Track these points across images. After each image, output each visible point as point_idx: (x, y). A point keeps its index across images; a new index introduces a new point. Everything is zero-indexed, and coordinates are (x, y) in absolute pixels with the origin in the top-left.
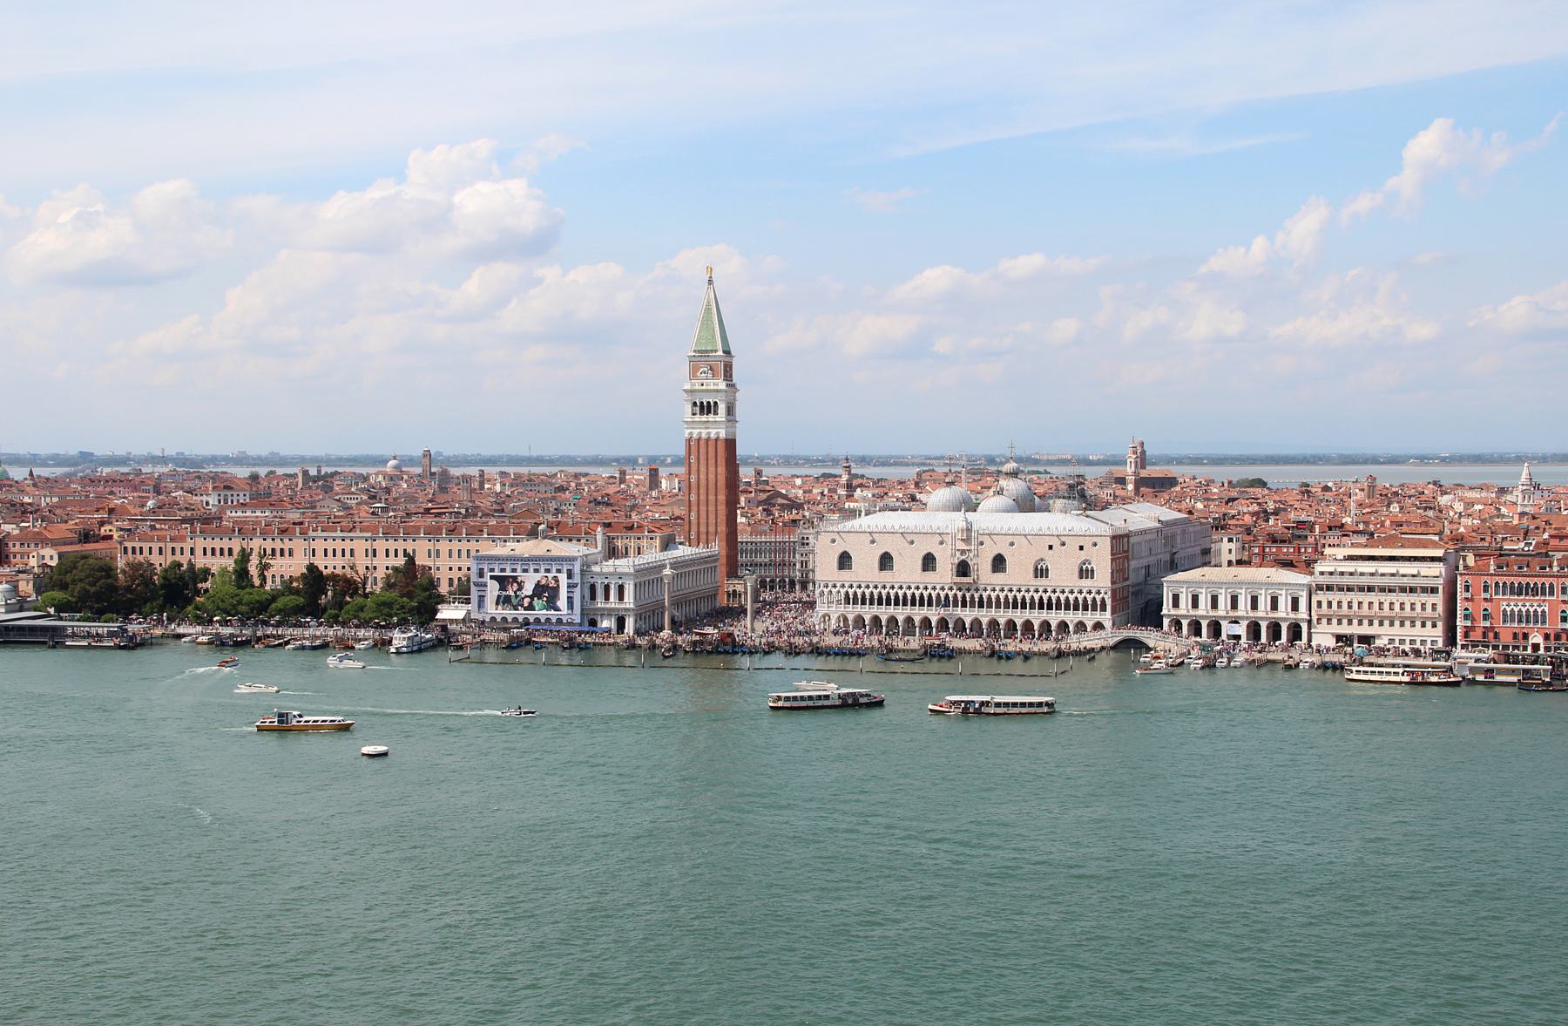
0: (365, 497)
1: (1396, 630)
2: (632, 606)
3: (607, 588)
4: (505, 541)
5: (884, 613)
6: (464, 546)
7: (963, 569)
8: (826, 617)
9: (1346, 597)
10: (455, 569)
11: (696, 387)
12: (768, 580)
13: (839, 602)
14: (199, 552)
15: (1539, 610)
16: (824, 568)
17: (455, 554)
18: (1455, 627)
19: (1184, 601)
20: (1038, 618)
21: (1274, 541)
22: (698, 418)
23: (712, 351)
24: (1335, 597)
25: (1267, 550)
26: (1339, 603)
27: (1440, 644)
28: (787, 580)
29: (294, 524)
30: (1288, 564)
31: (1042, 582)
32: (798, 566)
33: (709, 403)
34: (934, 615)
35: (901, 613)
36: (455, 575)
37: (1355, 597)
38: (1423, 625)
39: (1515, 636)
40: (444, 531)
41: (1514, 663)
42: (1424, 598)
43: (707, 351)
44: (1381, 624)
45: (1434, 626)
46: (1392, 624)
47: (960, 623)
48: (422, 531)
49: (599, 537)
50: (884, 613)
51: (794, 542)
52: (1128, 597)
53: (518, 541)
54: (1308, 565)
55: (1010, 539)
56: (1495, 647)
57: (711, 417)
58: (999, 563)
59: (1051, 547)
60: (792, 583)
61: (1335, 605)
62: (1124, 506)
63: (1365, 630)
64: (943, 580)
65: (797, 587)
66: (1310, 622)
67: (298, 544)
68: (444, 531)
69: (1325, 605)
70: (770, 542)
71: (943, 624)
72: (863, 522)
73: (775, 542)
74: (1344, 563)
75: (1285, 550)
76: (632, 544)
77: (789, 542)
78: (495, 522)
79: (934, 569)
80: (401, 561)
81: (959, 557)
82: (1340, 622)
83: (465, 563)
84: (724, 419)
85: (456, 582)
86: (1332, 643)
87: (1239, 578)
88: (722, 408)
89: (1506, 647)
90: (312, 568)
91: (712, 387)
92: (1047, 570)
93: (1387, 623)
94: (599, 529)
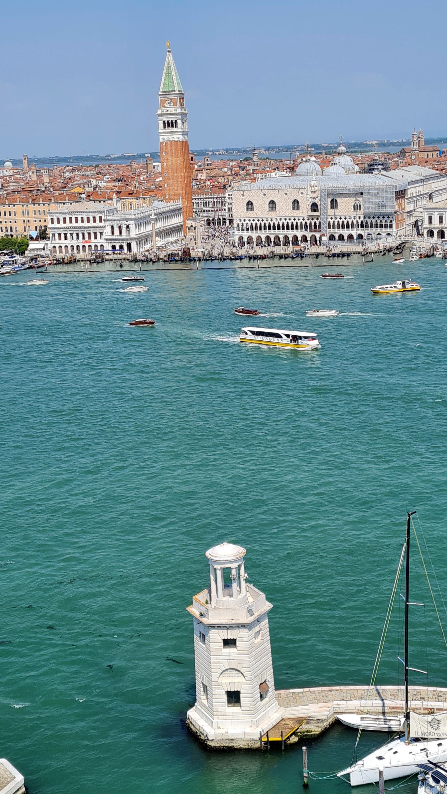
2: (135, 237)
4: (64, 204)
5: (272, 234)
6: (42, 207)
7: (314, 207)
8: (241, 238)
10: (38, 221)
11: (165, 112)
12: (211, 219)
13: (247, 229)
17: (37, 213)
19: (436, 220)
20: (356, 233)
23: (171, 91)
28: (221, 218)
32: (227, 210)
33: (172, 121)
34: (299, 234)
35: (281, 234)
36: (38, 224)
40: (30, 200)
43: (170, 91)
47: (313, 237)
49: (115, 200)
50: (272, 234)
51: (224, 197)
52: (404, 219)
53: (71, 204)
57: (174, 129)
62: (403, 168)
64: (303, 215)
65: (227, 222)
68: (30, 200)
70: (211, 198)
71: (305, 239)
72: (259, 184)
73: (214, 198)
77: (222, 197)
78: (57, 194)
79: (298, 208)
81: (311, 201)
83: (42, 217)
84: (181, 130)
85: (38, 228)
88: (179, 122)
91: (173, 112)
94: (115, 195)
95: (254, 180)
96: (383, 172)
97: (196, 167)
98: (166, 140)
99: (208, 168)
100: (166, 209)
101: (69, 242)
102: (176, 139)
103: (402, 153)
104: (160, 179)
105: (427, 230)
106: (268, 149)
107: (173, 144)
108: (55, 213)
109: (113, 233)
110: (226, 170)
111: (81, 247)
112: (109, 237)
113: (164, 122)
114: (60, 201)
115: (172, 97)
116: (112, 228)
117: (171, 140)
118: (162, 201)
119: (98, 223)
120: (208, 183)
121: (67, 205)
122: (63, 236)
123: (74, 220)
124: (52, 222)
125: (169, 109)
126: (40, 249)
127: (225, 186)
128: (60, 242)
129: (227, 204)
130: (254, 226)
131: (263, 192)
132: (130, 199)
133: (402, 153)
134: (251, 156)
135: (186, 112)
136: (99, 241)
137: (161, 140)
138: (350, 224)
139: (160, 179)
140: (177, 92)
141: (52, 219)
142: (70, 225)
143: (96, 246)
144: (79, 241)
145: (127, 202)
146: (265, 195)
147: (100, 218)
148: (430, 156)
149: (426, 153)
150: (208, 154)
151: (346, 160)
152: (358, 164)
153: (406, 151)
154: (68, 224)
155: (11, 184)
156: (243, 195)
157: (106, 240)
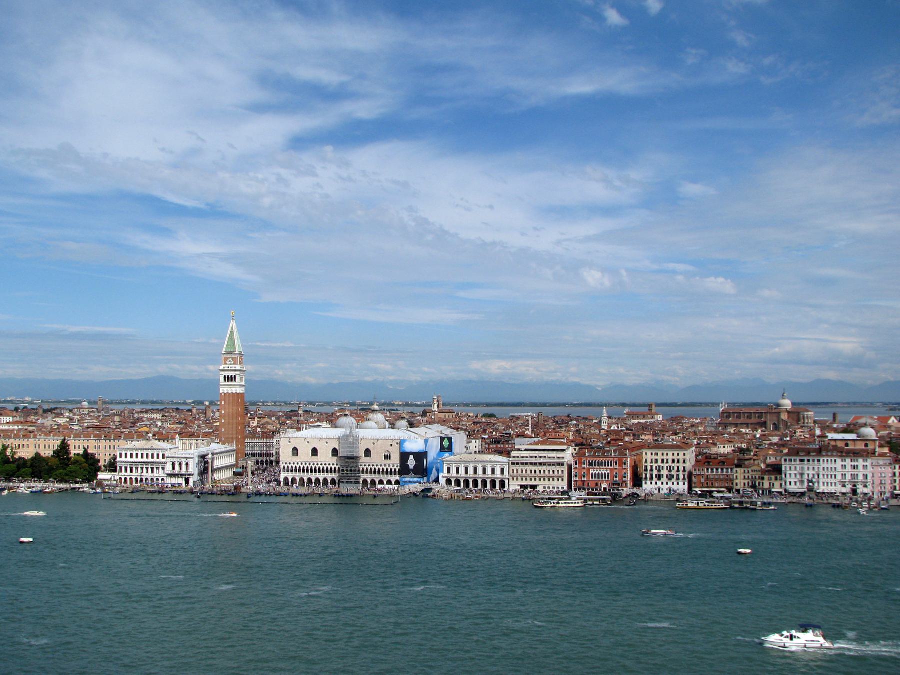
0: (68, 420)
1: (547, 483)
3: (180, 464)
5: (314, 476)
8: (286, 479)
9: (525, 468)
10: (108, 455)
14: (42, 447)
15: (607, 473)
16: (286, 457)
18: (572, 481)
21: (495, 443)
22: (227, 383)
23: (234, 352)
24: (520, 468)
25: (492, 446)
26: (522, 471)
27: (566, 488)
29: (31, 433)
30: (500, 453)
31: (388, 461)
33: (232, 376)
35: (321, 477)
36: (108, 458)
37: (529, 468)
38: (558, 480)
39: (597, 485)
40: (103, 437)
41: (597, 496)
42: (558, 468)
43: (231, 352)
44: (540, 480)
45: (563, 480)
46: (545, 480)
48: (92, 436)
51: (273, 443)
54: (508, 454)
55: (373, 441)
56: (588, 490)
57: (233, 383)
58: (368, 453)
59: (392, 445)
60: (272, 462)
61: (520, 472)
62: (426, 426)
63: (533, 483)
66: (509, 479)
67: (31, 442)
69: (515, 472)
72: (305, 433)
74: (525, 452)
75: (500, 446)
76: (194, 442)
77: (270, 443)
80: (81, 452)
82: (522, 480)
86: (519, 488)
87: (477, 459)
88: (238, 378)
89: (593, 490)
90: (38, 454)
91: (233, 369)
92: (390, 456)
93: (542, 479)
94: (178, 436)
95: (299, 429)
96: (409, 429)
97: (249, 415)
98: (226, 392)
99: (260, 416)
100: (220, 451)
101: (135, 474)
102: (234, 392)
103: (424, 414)
104: (218, 424)
105: (463, 479)
106: (312, 403)
107: (231, 395)
108: (124, 449)
109: (174, 468)
110: (275, 418)
111: (129, 480)
112: (170, 473)
113: (225, 377)
114: (130, 437)
115: (233, 356)
116: (173, 464)
117: (230, 392)
118: (218, 443)
119: (161, 460)
120: (259, 430)
121: (135, 443)
122: (129, 470)
123: (140, 456)
124: (121, 457)
125: (230, 366)
126: (107, 480)
127: (273, 433)
128: (126, 474)
129: (275, 449)
130: (298, 469)
131: (307, 440)
132: (191, 440)
133: (424, 414)
134: (297, 409)
135: (245, 369)
136: (159, 474)
137: (221, 391)
138: (381, 471)
139: (218, 424)
140: (237, 353)
141: (121, 454)
142: (136, 460)
143: (147, 479)
144: (143, 474)
145: (188, 442)
146: (308, 442)
147: (164, 455)
148: (447, 417)
149: (444, 414)
150: (259, 405)
151: (380, 417)
152: (387, 421)
153: (428, 411)
154: (134, 459)
155: (86, 421)
156: (290, 442)
157: (168, 475)
